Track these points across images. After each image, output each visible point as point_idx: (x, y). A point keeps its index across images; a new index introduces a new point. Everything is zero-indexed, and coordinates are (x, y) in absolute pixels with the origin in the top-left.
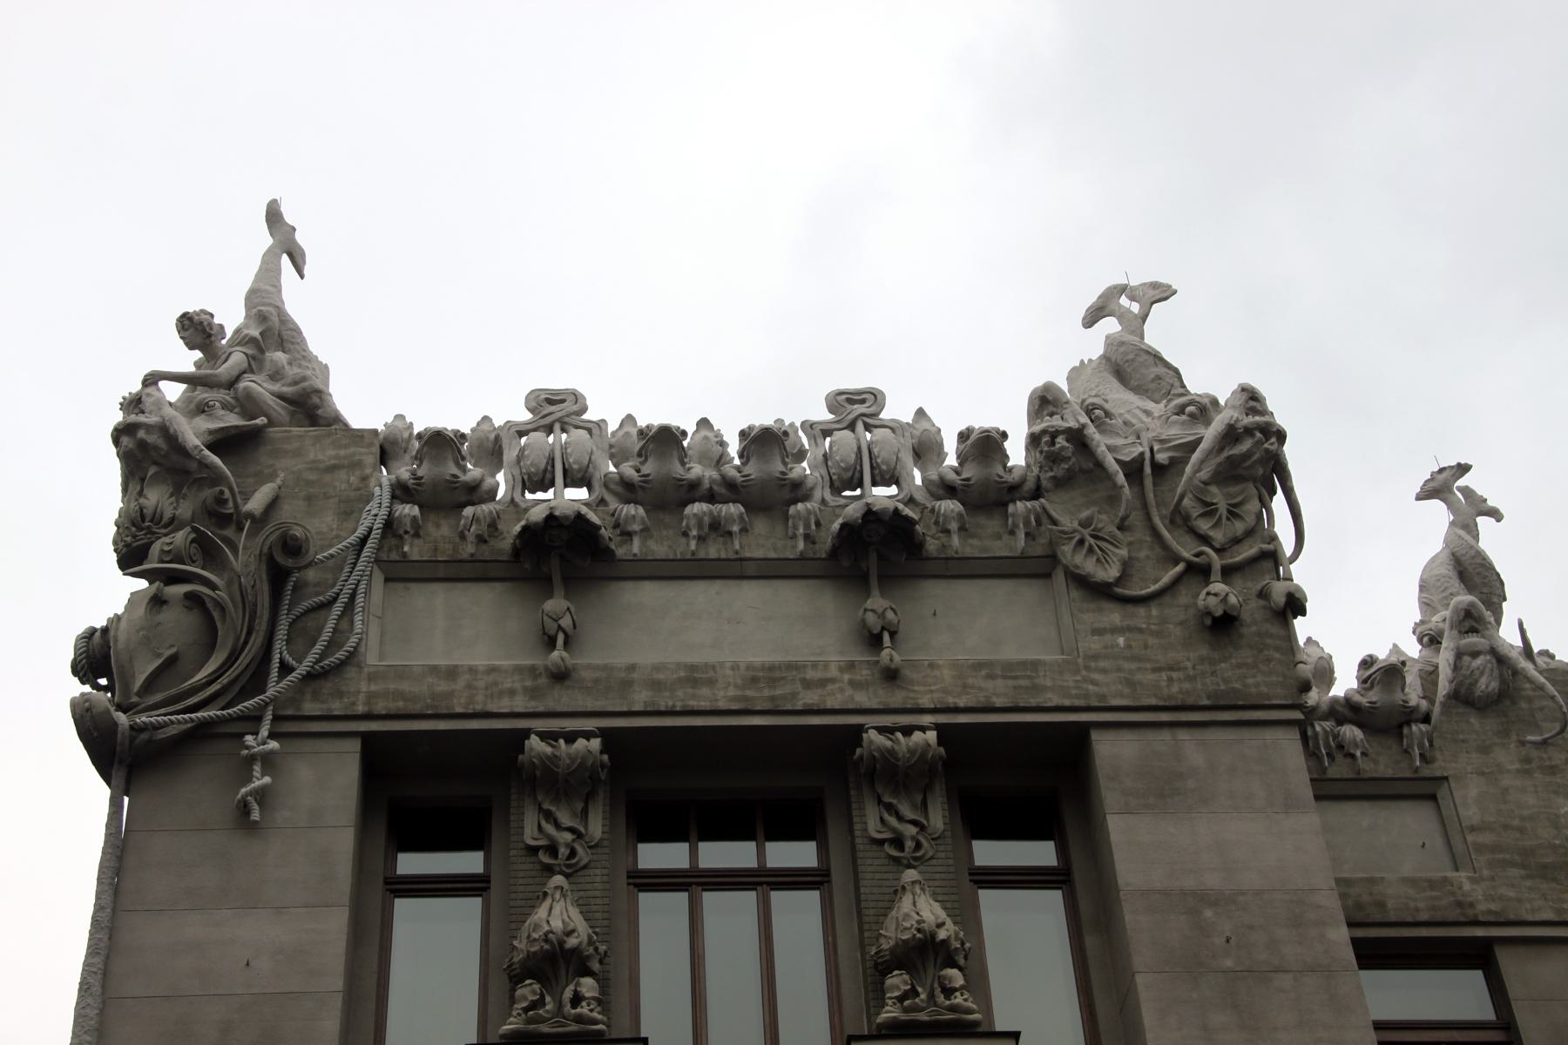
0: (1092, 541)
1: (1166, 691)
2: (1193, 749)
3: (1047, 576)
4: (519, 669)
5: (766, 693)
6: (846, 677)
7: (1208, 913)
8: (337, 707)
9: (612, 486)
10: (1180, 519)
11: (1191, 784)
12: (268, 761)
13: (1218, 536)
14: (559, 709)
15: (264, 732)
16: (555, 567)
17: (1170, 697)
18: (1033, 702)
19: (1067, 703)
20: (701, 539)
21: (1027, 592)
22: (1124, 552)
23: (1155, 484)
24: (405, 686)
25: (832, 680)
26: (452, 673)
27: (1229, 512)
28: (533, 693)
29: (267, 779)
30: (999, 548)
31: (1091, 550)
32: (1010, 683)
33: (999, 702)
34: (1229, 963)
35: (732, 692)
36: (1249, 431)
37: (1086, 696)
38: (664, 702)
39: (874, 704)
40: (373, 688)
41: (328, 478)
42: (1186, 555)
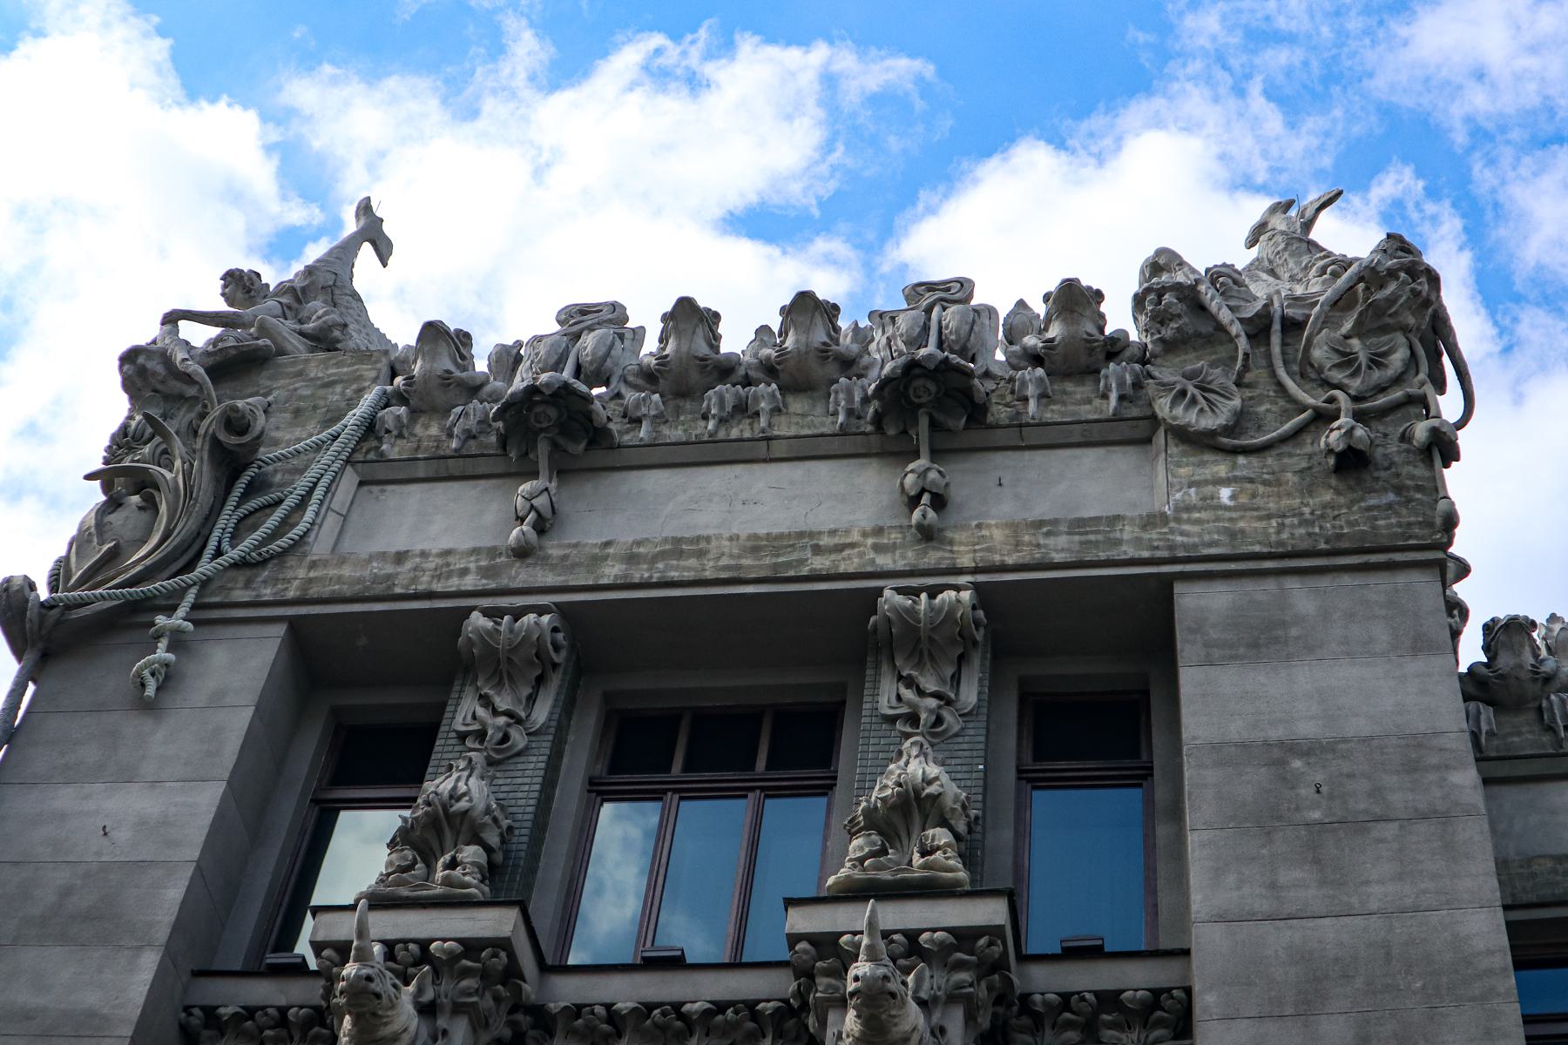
0: (1196, 392)
1: (1273, 538)
2: (1302, 597)
3: (1148, 441)
4: (475, 551)
5: (767, 561)
6: (870, 541)
7: (1297, 764)
8: (267, 593)
9: (631, 378)
10: (1308, 372)
11: (1294, 632)
12: (178, 642)
13: (1355, 384)
14: (513, 585)
15: (181, 612)
16: (543, 449)
17: (1280, 543)
18: (1103, 556)
19: (1146, 554)
20: (722, 421)
21: (1122, 460)
22: (1236, 402)
23: (1284, 344)
24: (347, 571)
25: (852, 545)
26: (400, 557)
27: (1372, 360)
28: (485, 572)
29: (171, 657)
30: (1086, 412)
31: (1194, 401)
32: (1077, 538)
33: (1058, 557)
34: (1316, 815)
35: (725, 561)
36: (1392, 274)
37: (1171, 548)
38: (640, 573)
39: (901, 565)
40: (312, 574)
41: (322, 392)
42: (1311, 401)
